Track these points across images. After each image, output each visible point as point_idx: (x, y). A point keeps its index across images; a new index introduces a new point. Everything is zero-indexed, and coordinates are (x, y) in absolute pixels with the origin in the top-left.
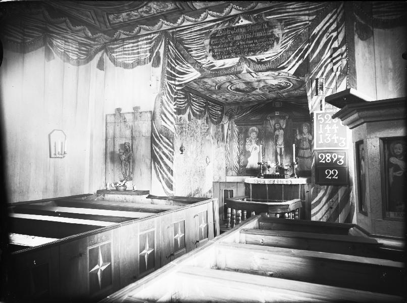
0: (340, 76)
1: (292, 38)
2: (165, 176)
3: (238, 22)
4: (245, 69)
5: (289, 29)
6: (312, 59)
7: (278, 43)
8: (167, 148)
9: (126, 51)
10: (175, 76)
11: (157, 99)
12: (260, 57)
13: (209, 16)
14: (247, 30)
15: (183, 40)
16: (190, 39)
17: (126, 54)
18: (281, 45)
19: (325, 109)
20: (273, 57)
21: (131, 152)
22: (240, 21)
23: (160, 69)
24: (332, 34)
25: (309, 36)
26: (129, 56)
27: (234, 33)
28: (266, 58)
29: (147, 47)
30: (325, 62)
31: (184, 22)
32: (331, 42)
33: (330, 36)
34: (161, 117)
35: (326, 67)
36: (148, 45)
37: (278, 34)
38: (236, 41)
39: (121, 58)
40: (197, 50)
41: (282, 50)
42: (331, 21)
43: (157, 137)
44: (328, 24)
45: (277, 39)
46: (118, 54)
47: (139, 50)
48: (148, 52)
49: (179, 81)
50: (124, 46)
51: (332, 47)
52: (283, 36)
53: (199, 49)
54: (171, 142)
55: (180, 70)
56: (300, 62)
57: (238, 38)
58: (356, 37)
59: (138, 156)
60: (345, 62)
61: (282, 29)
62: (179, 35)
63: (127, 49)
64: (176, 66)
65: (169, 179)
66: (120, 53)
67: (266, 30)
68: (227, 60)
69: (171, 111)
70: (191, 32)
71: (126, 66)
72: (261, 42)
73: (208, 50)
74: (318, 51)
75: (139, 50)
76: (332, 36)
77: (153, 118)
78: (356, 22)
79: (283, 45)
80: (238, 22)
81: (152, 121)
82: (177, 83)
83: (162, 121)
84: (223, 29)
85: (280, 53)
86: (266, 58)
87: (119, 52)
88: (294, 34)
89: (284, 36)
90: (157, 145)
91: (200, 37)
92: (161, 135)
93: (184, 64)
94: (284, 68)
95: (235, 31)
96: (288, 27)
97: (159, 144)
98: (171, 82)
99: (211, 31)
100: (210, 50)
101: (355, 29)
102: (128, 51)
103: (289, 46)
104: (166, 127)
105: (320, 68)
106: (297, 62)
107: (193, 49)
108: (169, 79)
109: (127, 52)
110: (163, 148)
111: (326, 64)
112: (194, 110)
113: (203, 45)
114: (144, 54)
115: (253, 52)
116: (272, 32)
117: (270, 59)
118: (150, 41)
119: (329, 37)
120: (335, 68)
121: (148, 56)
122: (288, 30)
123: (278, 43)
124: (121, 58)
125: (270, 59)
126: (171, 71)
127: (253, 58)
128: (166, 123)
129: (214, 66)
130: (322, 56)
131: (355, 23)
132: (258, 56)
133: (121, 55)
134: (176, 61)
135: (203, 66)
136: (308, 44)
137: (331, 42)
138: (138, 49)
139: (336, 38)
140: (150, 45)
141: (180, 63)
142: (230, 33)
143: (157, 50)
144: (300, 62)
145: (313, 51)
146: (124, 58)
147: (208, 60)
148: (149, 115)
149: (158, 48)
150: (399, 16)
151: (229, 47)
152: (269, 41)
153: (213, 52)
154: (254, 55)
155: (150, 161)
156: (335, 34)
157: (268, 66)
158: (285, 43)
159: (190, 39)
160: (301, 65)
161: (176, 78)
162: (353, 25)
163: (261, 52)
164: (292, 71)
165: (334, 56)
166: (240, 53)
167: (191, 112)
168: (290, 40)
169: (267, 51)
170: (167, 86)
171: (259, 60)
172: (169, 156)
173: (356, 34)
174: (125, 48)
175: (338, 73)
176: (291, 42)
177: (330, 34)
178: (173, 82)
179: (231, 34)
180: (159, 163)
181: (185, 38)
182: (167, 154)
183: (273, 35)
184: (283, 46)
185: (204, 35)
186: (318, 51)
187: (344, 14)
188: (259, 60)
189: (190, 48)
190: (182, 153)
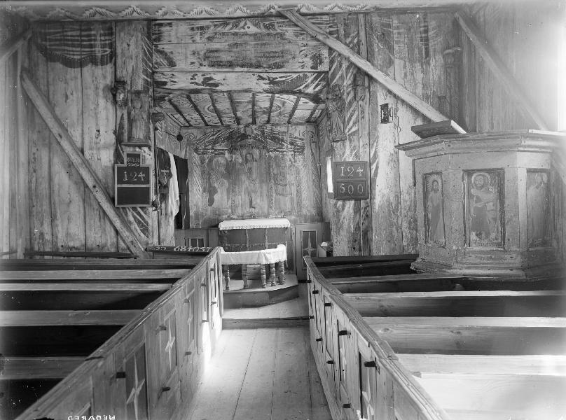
3: (243, 28)
9: (69, 40)
13: (204, 12)
17: (68, 45)
22: (246, 27)
26: (74, 49)
28: (280, 77)
29: (106, 40)
31: (166, 14)
36: (107, 38)
39: (59, 50)
46: (52, 43)
47: (93, 43)
48: (108, 46)
50: (65, 34)
63: (69, 38)
66: (57, 43)
71: (69, 63)
75: (93, 43)
80: (243, 28)
86: (280, 77)
87: (56, 40)
102: (72, 40)
109: (70, 43)
117: (284, 79)
124: (59, 50)
125: (284, 79)
129: (211, 79)
133: (58, 45)
138: (90, 40)
140: (110, 38)
146: (64, 50)
174: (68, 36)
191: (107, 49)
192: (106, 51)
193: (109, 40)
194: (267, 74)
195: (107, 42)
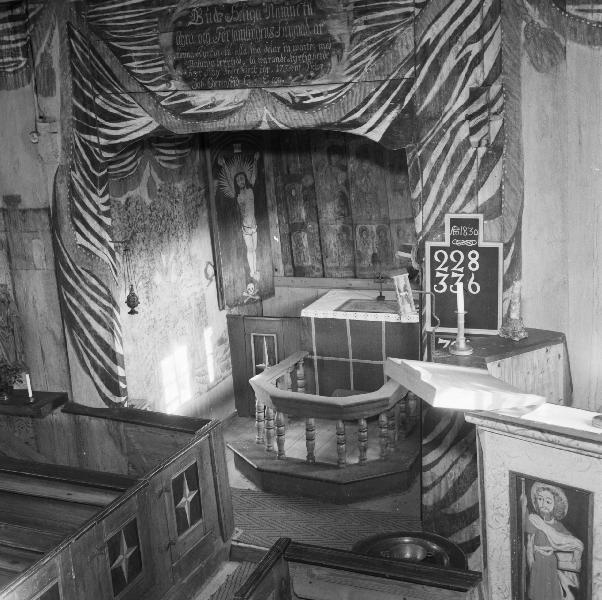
1: (373, 48)
2: (99, 363)
4: (264, 119)
5: (366, 23)
6: (423, 106)
7: (339, 58)
8: (96, 301)
10: (94, 122)
11: (57, 180)
12: (301, 91)
14: (263, 16)
15: (107, 28)
16: (122, 27)
18: (347, 65)
19: (452, 237)
20: (330, 95)
21: (13, 306)
23: (53, 105)
24: (469, 48)
25: (416, 47)
27: (233, 23)
30: (453, 118)
32: (466, 68)
33: (464, 52)
34: (74, 223)
35: (454, 132)
36: (18, 36)
37: (340, 36)
38: (239, 43)
40: (142, 58)
43: (69, 271)
44: (460, 20)
45: (339, 46)
48: (21, 53)
49: (107, 137)
51: (471, 83)
53: (149, 57)
54: (103, 285)
55: (106, 107)
56: (394, 113)
57: (244, 35)
58: (525, 61)
59: (31, 314)
60: (496, 125)
61: (350, 23)
62: (95, 13)
64: (96, 96)
65: (110, 369)
67: (311, 20)
68: (220, 92)
69: (95, 211)
70: (123, 8)
73: (171, 62)
74: (435, 89)
76: (469, 54)
77: (55, 228)
78: (525, 20)
79: (352, 65)
81: (52, 231)
82: (103, 141)
83: (78, 235)
84: (204, 8)
85: (347, 84)
89: (354, 41)
90: (72, 291)
91: (146, 24)
92: (79, 268)
93: (117, 94)
94: (356, 124)
95: (235, 15)
96: (364, 18)
97: (80, 291)
98: (86, 137)
99: (174, 11)
100: (176, 63)
101: (523, 39)
103: (366, 69)
104: (87, 250)
105: (441, 134)
106: (388, 111)
107: (134, 54)
108: (83, 129)
110: (87, 299)
111: (454, 125)
112: (164, 165)
113: (157, 47)
114: (10, 59)
116: (325, 28)
117: (322, 98)
118: (21, 23)
120: (474, 139)
121: (23, 64)
122: (363, 27)
123: (339, 58)
125: (322, 98)
126: (84, 109)
127: (283, 92)
128: (88, 240)
129: (188, 105)
132: (296, 89)
134: (94, 84)
135: (163, 103)
136: (413, 69)
137: (466, 68)
139: (479, 58)
141: (105, 89)
142: (223, 19)
143: (42, 50)
144: (394, 113)
145: (425, 88)
147: (173, 88)
148: (45, 218)
149: (44, 45)
151: (223, 58)
152: (318, 51)
153: (184, 67)
154: (285, 85)
155: (60, 328)
156: (475, 48)
159: (122, 27)
160: (396, 123)
161: (100, 129)
162: (519, 28)
163: (300, 80)
166: (252, 78)
167: (155, 175)
168: (367, 53)
169: (314, 78)
170: (82, 150)
171: (297, 100)
172: (102, 316)
173: (526, 54)
175: (482, 151)
176: (371, 58)
177: (464, 47)
178: (94, 139)
179: (224, 23)
180: (81, 332)
181: (108, 21)
182: (100, 314)
183: (326, 38)
185: (156, 20)
186: (435, 89)
188: (297, 100)
189: (126, 51)
190: (132, 312)
191: (21, 58)
192: (21, 62)
193: (22, 40)
194: (288, 90)
195: (19, 45)
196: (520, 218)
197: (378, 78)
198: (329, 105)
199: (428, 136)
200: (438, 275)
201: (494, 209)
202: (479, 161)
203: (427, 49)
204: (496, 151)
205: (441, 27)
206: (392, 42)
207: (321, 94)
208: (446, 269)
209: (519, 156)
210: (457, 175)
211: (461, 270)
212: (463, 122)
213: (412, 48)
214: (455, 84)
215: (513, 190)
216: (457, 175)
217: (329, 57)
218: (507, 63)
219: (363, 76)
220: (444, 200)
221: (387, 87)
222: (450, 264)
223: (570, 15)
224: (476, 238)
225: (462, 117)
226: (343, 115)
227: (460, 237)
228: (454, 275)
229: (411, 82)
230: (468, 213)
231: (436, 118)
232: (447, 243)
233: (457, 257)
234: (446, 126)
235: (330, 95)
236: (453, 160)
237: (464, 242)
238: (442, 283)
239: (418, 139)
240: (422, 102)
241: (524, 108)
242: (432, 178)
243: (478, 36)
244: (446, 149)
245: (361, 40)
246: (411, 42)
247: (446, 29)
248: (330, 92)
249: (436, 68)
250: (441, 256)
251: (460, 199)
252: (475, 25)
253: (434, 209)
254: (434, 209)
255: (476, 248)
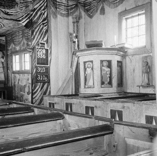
0: (45, 32)
1: (25, 6)
6: (34, 20)
7: (17, 6)
12: (7, 11)
18: (19, 8)
19: (40, 46)
20: (14, 13)
30: (40, 24)
32: (42, 15)
35: (40, 26)
37: (18, 1)
41: (19, 11)
42: (42, 5)
44: (41, 6)
45: (17, 4)
52: (20, 3)
56: (28, 20)
58: (52, 16)
72: (8, 2)
76: (42, 12)
79: (20, 8)
85: (18, 12)
88: (26, 4)
94: (20, 21)
103: (23, 10)
105: (38, 26)
106: (27, 19)
111: (40, 25)
115: (3, 6)
119: (41, 12)
123: (17, 6)
127: (3, 10)
130: (39, 20)
131: (51, 10)
132: (6, 10)
137: (42, 15)
139: (44, 14)
144: (28, 20)
145: (34, 16)
150: (65, 13)
152: (12, 3)
154: (4, 8)
157: (12, 17)
158: (21, 8)
160: (28, 22)
163: (8, 8)
164: (24, 24)
165: (44, 22)
168: (24, 7)
169: (11, 9)
171: (6, 12)
175: (45, 31)
176: (24, 8)
177: (42, 11)
184: (20, 9)
187: (47, 3)
188: (6, 12)
194: (5, 10)
196: (51, 44)
197: (25, 12)
198: (14, 15)
199: (35, 26)
200: (38, 54)
201: (47, 41)
202: (44, 33)
203: (35, 9)
204: (47, 31)
205: (38, 6)
206: (28, 6)
207: (12, 12)
208: (39, 53)
209: (51, 32)
210: (41, 34)
211: (42, 53)
212: (42, 25)
213: (32, 8)
214: (40, 17)
215: (50, 39)
216: (41, 34)
217: (15, 5)
218: (48, 16)
219: (22, 11)
220: (38, 39)
221: (27, 15)
222: (40, 52)
223: (58, 11)
224: (44, 47)
225: (41, 24)
226: (17, 18)
227: (42, 47)
228: (41, 54)
229: (32, 15)
230: (42, 42)
231: (37, 23)
232: (39, 47)
233: (41, 50)
234: (39, 25)
235: (14, 13)
236: (40, 32)
237: (42, 48)
238: (39, 55)
239: (33, 26)
240: (34, 19)
241: (52, 24)
242: (36, 34)
243: (44, 10)
244: (39, 29)
245: (22, 4)
246: (32, 7)
247: (39, 6)
248: (14, 13)
249: (37, 13)
250: (38, 50)
251: (41, 39)
252: (43, 8)
253: (36, 40)
254: (36, 40)
255: (45, 49)
